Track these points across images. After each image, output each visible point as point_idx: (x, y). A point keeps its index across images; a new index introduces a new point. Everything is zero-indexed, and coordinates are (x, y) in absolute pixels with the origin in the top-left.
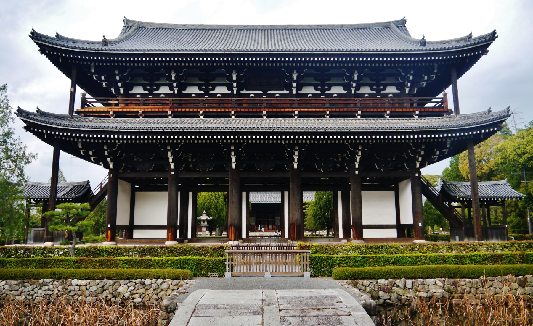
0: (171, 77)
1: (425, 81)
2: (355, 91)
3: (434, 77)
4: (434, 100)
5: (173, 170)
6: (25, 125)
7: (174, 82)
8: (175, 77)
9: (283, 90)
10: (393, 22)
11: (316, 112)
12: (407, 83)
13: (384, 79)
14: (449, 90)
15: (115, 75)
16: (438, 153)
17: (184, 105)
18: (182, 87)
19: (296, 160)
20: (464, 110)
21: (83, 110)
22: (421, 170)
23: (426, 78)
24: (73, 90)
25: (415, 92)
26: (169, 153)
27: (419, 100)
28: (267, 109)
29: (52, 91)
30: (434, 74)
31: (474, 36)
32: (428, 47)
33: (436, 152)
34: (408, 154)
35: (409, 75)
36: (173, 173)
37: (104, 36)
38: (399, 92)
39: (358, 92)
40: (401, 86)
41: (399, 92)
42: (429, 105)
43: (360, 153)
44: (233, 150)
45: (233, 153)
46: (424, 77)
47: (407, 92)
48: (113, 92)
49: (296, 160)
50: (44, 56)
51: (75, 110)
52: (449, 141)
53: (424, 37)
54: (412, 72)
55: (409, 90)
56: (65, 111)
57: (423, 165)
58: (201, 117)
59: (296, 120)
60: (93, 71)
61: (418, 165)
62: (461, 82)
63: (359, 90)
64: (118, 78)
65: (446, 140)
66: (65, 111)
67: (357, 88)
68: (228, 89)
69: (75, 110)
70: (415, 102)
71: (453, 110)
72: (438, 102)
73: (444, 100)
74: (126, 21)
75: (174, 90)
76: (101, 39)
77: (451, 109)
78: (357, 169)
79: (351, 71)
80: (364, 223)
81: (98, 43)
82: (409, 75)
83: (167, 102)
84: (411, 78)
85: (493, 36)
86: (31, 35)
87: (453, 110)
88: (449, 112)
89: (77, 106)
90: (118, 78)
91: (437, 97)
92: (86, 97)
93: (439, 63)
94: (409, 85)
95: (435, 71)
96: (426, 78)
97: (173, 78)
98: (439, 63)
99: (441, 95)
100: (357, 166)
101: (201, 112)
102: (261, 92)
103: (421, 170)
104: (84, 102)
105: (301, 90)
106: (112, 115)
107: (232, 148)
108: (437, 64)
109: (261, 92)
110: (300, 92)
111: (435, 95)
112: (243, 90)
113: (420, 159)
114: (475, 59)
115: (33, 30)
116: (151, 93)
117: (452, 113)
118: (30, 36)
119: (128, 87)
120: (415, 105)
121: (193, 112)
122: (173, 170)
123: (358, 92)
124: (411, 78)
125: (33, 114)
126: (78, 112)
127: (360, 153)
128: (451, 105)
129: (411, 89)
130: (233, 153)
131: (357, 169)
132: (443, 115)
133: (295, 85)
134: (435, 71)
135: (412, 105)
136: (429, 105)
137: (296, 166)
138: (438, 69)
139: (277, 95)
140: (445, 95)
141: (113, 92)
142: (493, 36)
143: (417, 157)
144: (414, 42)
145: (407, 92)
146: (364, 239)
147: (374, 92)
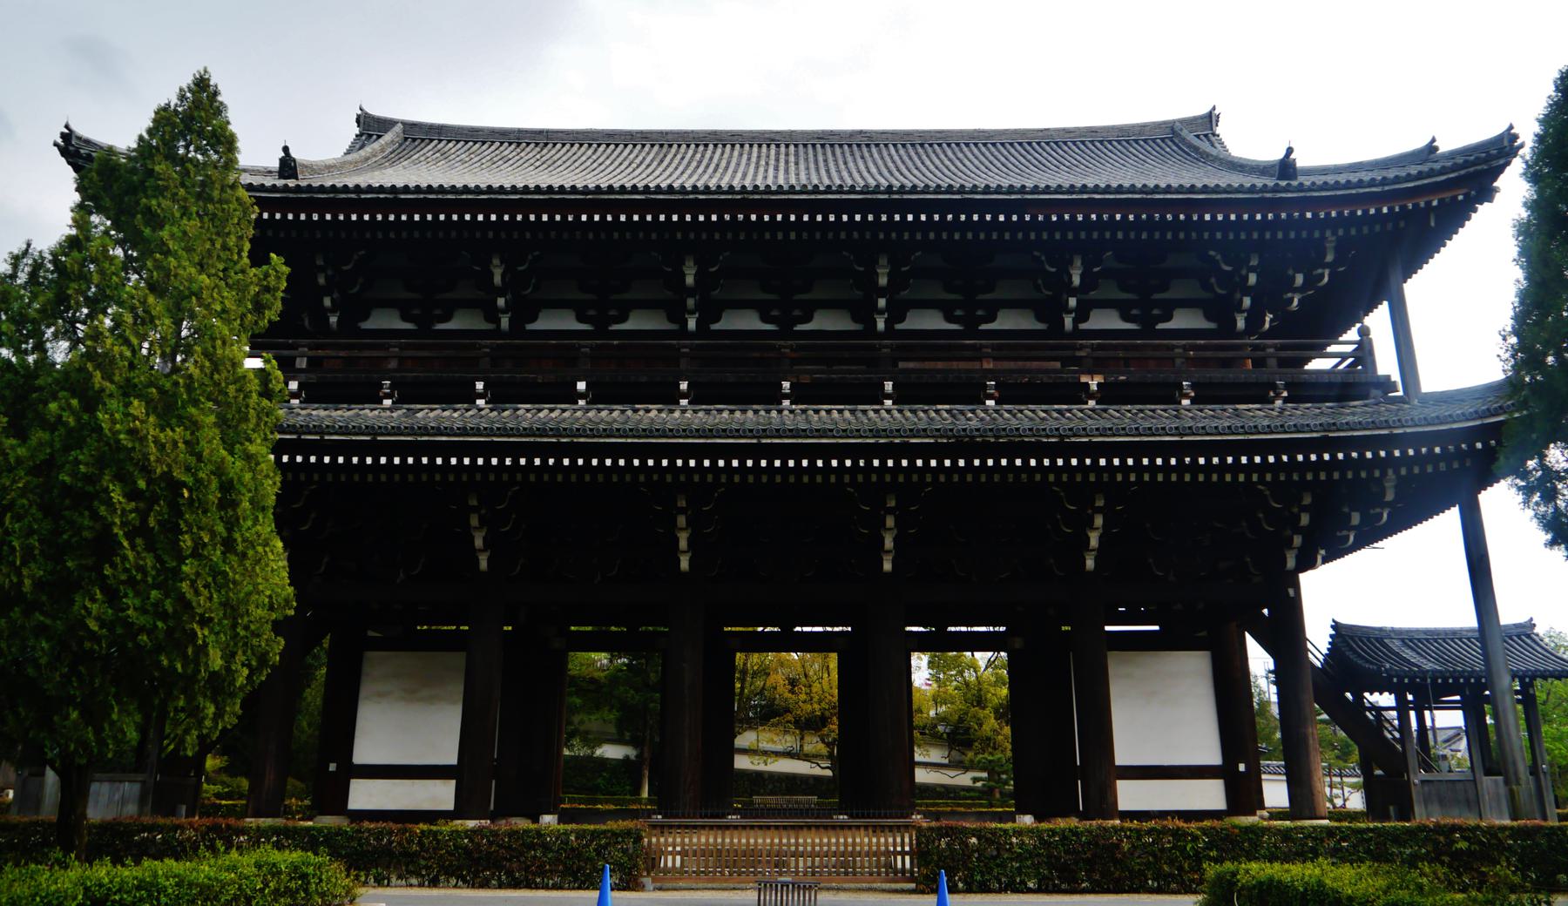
0: (492, 275)
1: (1296, 290)
2: (1076, 322)
3: (1326, 279)
4: (1332, 349)
7: (501, 292)
8: (503, 276)
13: (1164, 288)
14: (1379, 320)
16: (1356, 519)
18: (525, 311)
19: (889, 543)
20: (1431, 382)
25: (1267, 326)
26: (474, 521)
27: (1284, 348)
30: (1325, 266)
33: (1349, 518)
35: (1244, 272)
37: (286, 149)
39: (1083, 326)
40: (1221, 311)
42: (1317, 364)
43: (1099, 521)
44: (682, 511)
45: (682, 520)
46: (1293, 279)
47: (1241, 324)
48: (307, 323)
49: (889, 543)
53: (1290, 151)
54: (1254, 262)
59: (888, 411)
62: (1419, 289)
63: (1086, 319)
64: (322, 281)
65: (1384, 474)
67: (1082, 314)
68: (671, 319)
70: (1271, 356)
71: (1396, 377)
72: (1343, 357)
73: (1364, 351)
75: (498, 322)
77: (1388, 377)
80: (1121, 759)
82: (1244, 272)
84: (1252, 279)
86: (60, 141)
87: (1396, 377)
90: (322, 281)
91: (1344, 338)
93: (1341, 232)
94: (1247, 302)
95: (1329, 258)
97: (497, 279)
98: (1341, 232)
99: (1352, 334)
103: (1304, 578)
105: (902, 320)
108: (1334, 233)
110: (899, 327)
111: (1334, 334)
113: (1298, 540)
115: (67, 127)
117: (1394, 387)
118: (56, 144)
119: (354, 310)
120: (1272, 362)
123: (1083, 326)
124: (1252, 279)
127: (1099, 521)
128: (1386, 363)
129: (1254, 319)
130: (682, 520)
134: (1329, 258)
135: (1259, 363)
136: (1317, 364)
138: (1337, 250)
140: (1364, 332)
141: (307, 323)
143: (1288, 532)
145: (1241, 324)
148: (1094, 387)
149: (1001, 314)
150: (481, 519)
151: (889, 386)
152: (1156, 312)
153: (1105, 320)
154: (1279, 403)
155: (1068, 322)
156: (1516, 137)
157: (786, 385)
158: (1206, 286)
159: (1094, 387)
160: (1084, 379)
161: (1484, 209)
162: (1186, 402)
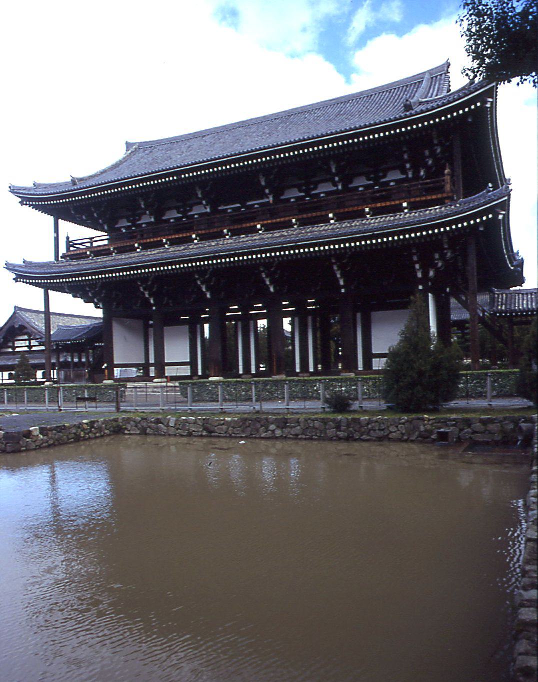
5: (154, 305)
6: (14, 276)
9: (262, 198)
11: (280, 222)
15: (92, 213)
17: (145, 236)
21: (69, 253)
24: (56, 236)
28: (228, 227)
29: (40, 238)
36: (154, 308)
50: (26, 208)
51: (60, 254)
52: (445, 239)
56: (51, 258)
58: (166, 246)
60: (73, 212)
66: (51, 258)
69: (60, 254)
74: (127, 143)
76: (69, 179)
78: (343, 287)
81: (66, 184)
83: (135, 234)
89: (63, 250)
90: (95, 215)
92: (70, 240)
96: (427, 153)
100: (342, 283)
101: (164, 241)
102: (238, 205)
104: (69, 243)
106: (90, 256)
109: (238, 205)
112: (220, 206)
116: (134, 225)
121: (158, 241)
122: (154, 305)
125: (20, 266)
126: (63, 257)
131: (343, 287)
132: (444, 203)
139: (256, 206)
147: (372, 182)
150: (144, 288)
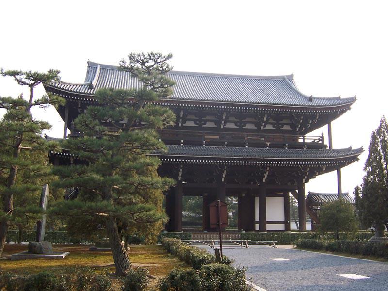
10: (286, 76)
12: (297, 124)
20: (335, 147)
22: (306, 185)
23: (311, 122)
31: (343, 97)
32: (315, 103)
34: (297, 173)
38: (292, 129)
41: (292, 129)
51: (67, 135)
54: (302, 118)
55: (299, 129)
57: (307, 181)
61: (304, 182)
69: (67, 135)
71: (328, 145)
79: (262, 115)
84: (301, 121)
85: (353, 100)
88: (326, 146)
94: (299, 126)
95: (317, 118)
96: (311, 122)
107: (182, 166)
114: (342, 112)
124: (301, 121)
128: (326, 142)
133: (223, 122)
137: (223, 180)
142: (353, 100)
144: (306, 97)
146: (268, 231)
148: (268, 144)
149: (247, 124)
151: (226, 143)
152: (280, 126)
153: (269, 127)
154: (305, 149)
155: (262, 127)
156: (356, 98)
157: (204, 142)
158: (291, 120)
159: (268, 144)
160: (266, 143)
161: (348, 111)
162: (286, 148)
